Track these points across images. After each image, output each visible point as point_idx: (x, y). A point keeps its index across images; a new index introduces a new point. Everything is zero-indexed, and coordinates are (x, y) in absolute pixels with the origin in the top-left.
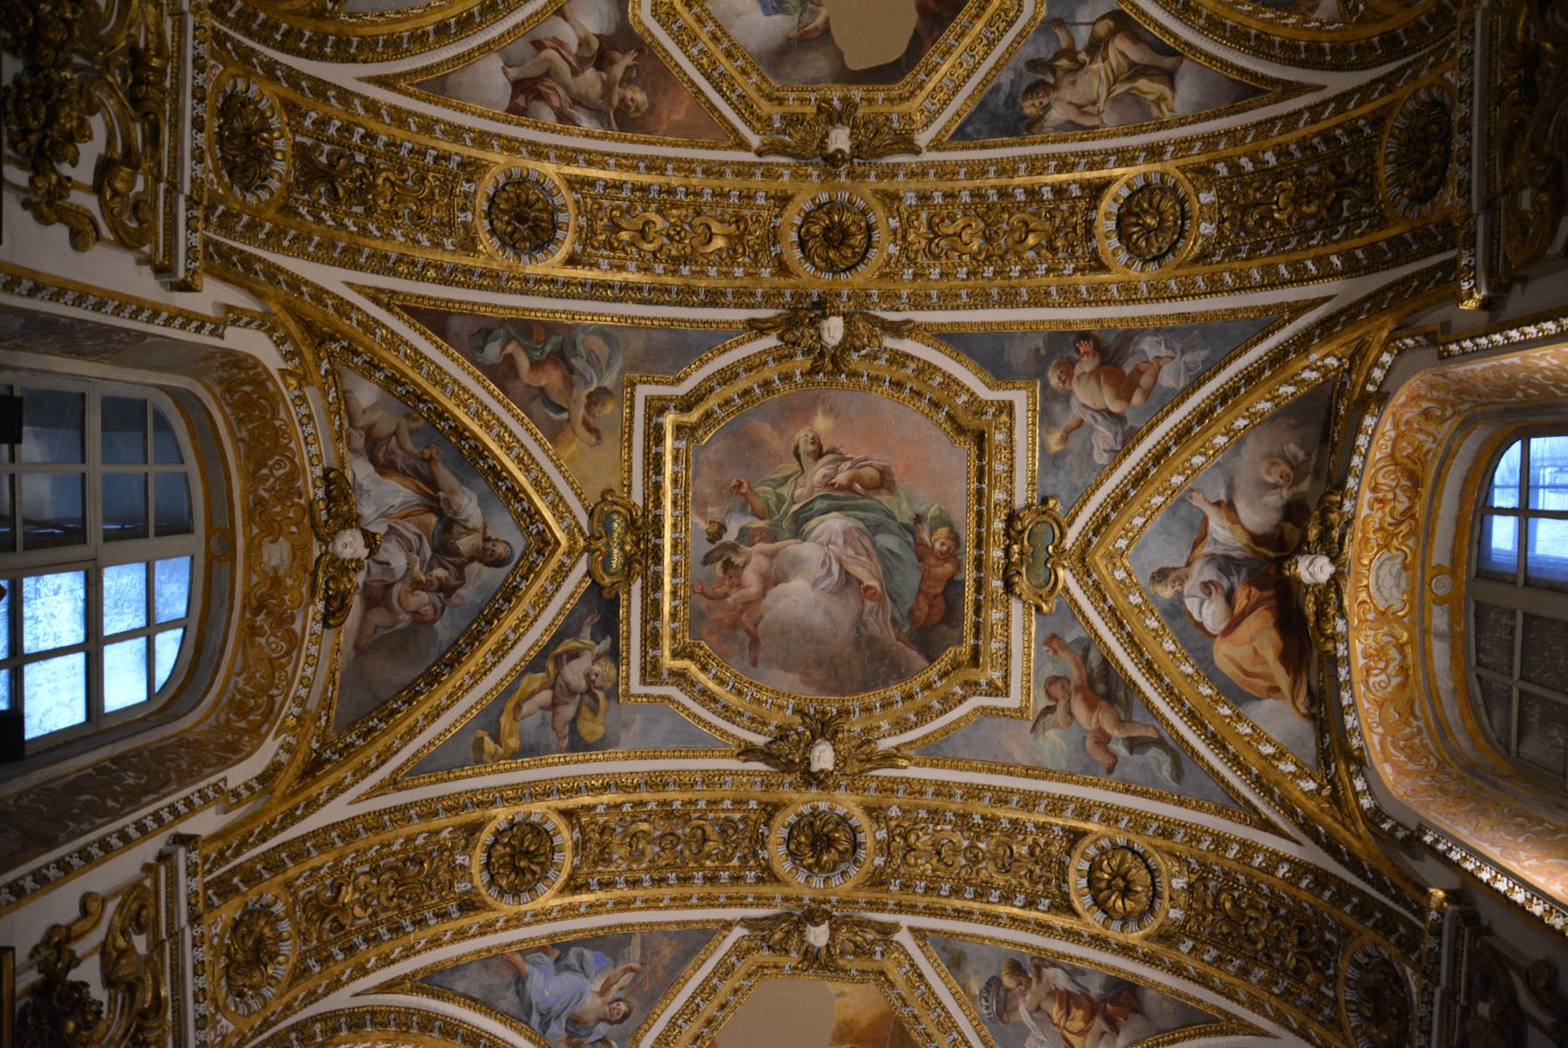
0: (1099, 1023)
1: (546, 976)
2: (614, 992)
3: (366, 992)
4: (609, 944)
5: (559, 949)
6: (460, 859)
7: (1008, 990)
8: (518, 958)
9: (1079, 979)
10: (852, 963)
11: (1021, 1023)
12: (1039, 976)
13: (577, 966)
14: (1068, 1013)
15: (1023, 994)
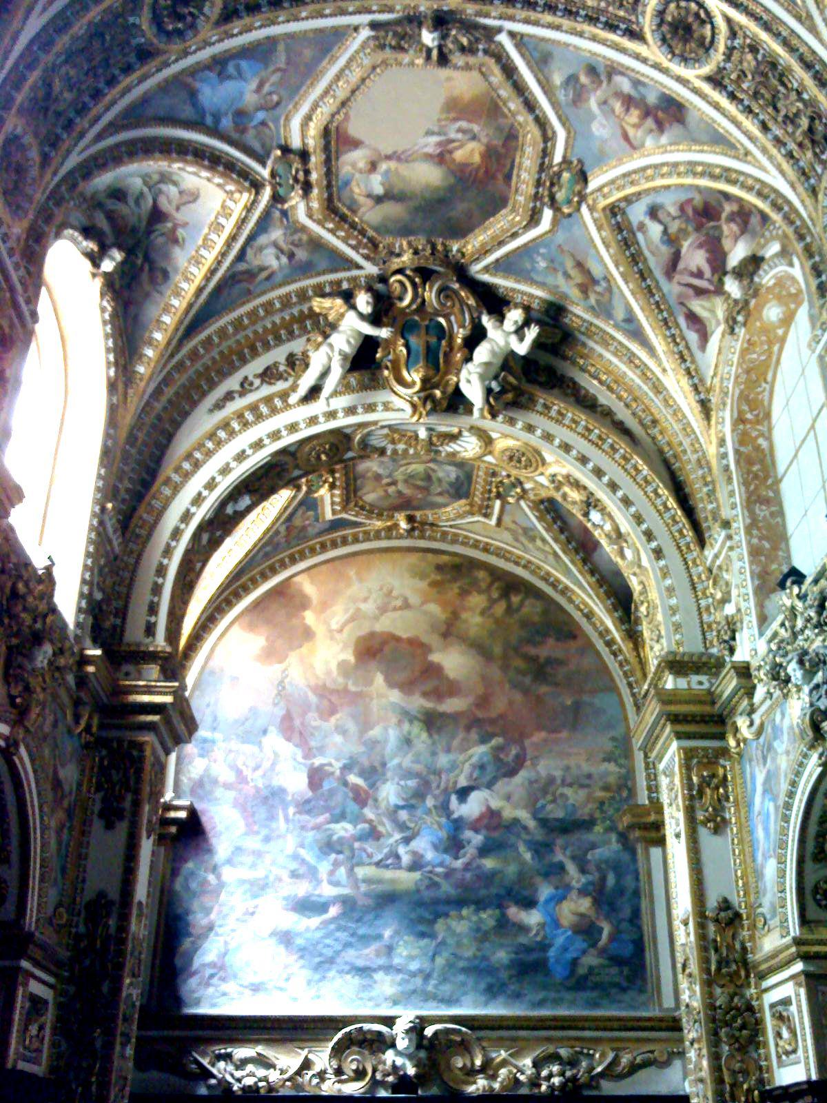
0: (650, 123)
1: (213, 87)
2: (267, 88)
3: (87, 147)
4: (260, 52)
5: (219, 65)
6: (131, 20)
7: (583, 86)
8: (190, 80)
9: (641, 89)
10: (458, 59)
11: (590, 109)
12: (609, 77)
13: (235, 73)
14: (628, 110)
15: (595, 90)
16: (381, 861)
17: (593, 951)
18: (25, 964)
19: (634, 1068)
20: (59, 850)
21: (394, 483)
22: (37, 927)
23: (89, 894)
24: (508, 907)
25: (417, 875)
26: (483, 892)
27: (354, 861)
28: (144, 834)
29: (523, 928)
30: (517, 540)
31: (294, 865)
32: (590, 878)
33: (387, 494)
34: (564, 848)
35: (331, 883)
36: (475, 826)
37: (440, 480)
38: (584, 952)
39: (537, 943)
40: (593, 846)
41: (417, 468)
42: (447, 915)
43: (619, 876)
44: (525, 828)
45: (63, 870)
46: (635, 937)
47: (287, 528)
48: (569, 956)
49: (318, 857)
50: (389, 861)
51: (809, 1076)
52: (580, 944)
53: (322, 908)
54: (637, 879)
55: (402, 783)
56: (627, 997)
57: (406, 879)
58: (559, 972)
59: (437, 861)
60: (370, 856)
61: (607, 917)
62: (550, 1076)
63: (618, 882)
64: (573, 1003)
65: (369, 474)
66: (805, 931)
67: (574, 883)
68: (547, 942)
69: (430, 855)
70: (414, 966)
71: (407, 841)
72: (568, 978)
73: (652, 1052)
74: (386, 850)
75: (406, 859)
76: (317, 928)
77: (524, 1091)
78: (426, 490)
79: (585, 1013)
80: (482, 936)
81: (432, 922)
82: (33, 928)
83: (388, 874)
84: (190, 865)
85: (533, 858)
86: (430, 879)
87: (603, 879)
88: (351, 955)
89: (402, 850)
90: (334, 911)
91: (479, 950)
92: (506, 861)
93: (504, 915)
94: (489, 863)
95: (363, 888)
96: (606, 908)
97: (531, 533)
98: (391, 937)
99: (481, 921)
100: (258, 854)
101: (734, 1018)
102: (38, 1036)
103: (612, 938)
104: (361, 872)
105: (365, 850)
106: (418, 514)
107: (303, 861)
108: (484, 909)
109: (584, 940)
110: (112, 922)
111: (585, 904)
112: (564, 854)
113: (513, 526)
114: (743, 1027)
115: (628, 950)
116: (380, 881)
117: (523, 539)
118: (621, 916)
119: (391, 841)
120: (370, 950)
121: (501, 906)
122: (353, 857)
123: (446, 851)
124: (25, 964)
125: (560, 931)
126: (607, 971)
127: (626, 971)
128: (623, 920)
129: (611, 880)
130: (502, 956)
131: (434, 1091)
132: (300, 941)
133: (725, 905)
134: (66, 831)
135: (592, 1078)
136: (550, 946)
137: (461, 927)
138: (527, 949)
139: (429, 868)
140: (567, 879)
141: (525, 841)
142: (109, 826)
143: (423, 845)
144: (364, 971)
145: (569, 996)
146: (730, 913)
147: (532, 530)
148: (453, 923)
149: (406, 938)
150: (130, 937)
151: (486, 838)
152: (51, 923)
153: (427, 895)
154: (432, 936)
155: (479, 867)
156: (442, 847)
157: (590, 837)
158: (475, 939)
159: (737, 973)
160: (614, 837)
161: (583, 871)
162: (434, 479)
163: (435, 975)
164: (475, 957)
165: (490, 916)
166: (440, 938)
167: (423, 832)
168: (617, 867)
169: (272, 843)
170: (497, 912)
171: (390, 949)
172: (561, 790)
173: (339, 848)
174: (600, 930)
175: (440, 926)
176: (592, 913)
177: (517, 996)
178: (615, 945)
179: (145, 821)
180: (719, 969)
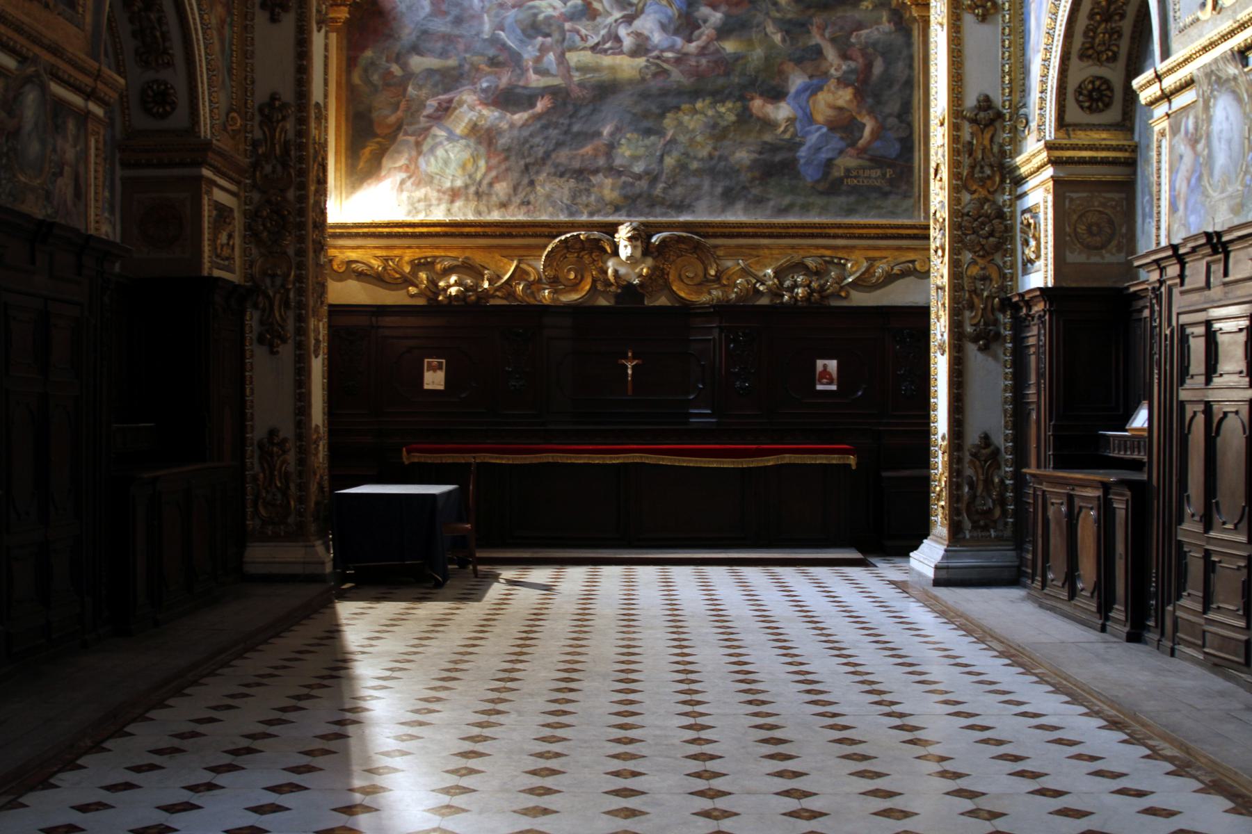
16: (598, 44)
17: (851, 151)
18: (206, 172)
19: (890, 278)
20: (223, 51)
22: (212, 133)
23: (261, 96)
24: (752, 99)
25: (641, 61)
26: (721, 81)
27: (566, 44)
28: (315, 27)
29: (769, 124)
31: (492, 52)
32: (853, 65)
34: (822, 29)
35: (537, 72)
38: (841, 152)
39: (788, 141)
40: (860, 26)
42: (678, 108)
43: (888, 64)
45: (230, 70)
46: (904, 135)
48: (824, 156)
49: (521, 41)
50: (608, 45)
51: (1046, 283)
52: (836, 142)
53: (528, 100)
54: (911, 67)
56: (889, 202)
57: (627, 66)
58: (810, 174)
59: (666, 44)
60: (584, 39)
61: (871, 112)
62: (795, 285)
63: (886, 70)
64: (824, 210)
66: (1062, 134)
67: (832, 71)
68: (798, 139)
69: (657, 37)
70: (638, 168)
71: (629, 20)
72: (818, 181)
73: (913, 262)
74: (603, 32)
75: (628, 42)
76: (523, 125)
77: (764, 301)
79: (839, 220)
80: (718, 133)
81: (662, 116)
82: (209, 137)
83: (607, 60)
84: (369, 53)
85: (784, 40)
86: (657, 65)
87: (869, 66)
88: (563, 156)
89: (623, 31)
90: (540, 106)
91: (715, 149)
92: (750, 42)
93: (746, 109)
94: (730, 47)
95: (577, 77)
96: (870, 101)
98: (612, 134)
99: (721, 116)
100: (449, 39)
101: (983, 224)
102: (228, 244)
103: (876, 135)
104: (573, 58)
105: (578, 32)
107: (504, 47)
108: (723, 102)
109: (842, 138)
110: (290, 125)
111: (845, 97)
112: (823, 35)
114: (991, 234)
115: (894, 150)
116: (597, 69)
118: (887, 110)
119: (610, 20)
120: (588, 149)
121: (742, 98)
122: (564, 39)
123: (676, 32)
124: (206, 172)
125: (814, 127)
126: (867, 173)
127: (889, 172)
128: (890, 115)
129: (878, 68)
130: (743, 156)
131: (663, 301)
132: (503, 141)
133: (986, 103)
134: (227, 28)
135: (842, 288)
136: (801, 144)
137: (693, 122)
138: (774, 148)
139: (655, 53)
140: (824, 66)
141: (775, 20)
142: (274, 19)
143: (648, 24)
144: (581, 174)
145: (821, 201)
146: (991, 113)
148: (686, 119)
149: (628, 135)
150: (311, 141)
151: (727, 16)
152: (225, 129)
153: (655, 85)
154: (660, 132)
155: (717, 51)
156: (672, 26)
157: (857, 15)
158: (712, 136)
159: (989, 177)
160: (885, 16)
161: (845, 56)
163: (664, 178)
164: (711, 157)
165: (729, 110)
166: (668, 138)
167: (648, 10)
168: (888, 52)
169: (465, 25)
170: (739, 104)
171: (611, 147)
173: (547, 31)
174: (864, 125)
175: (669, 121)
176: (853, 107)
177: (759, 201)
178: (877, 144)
179: (314, 10)
180: (971, 174)
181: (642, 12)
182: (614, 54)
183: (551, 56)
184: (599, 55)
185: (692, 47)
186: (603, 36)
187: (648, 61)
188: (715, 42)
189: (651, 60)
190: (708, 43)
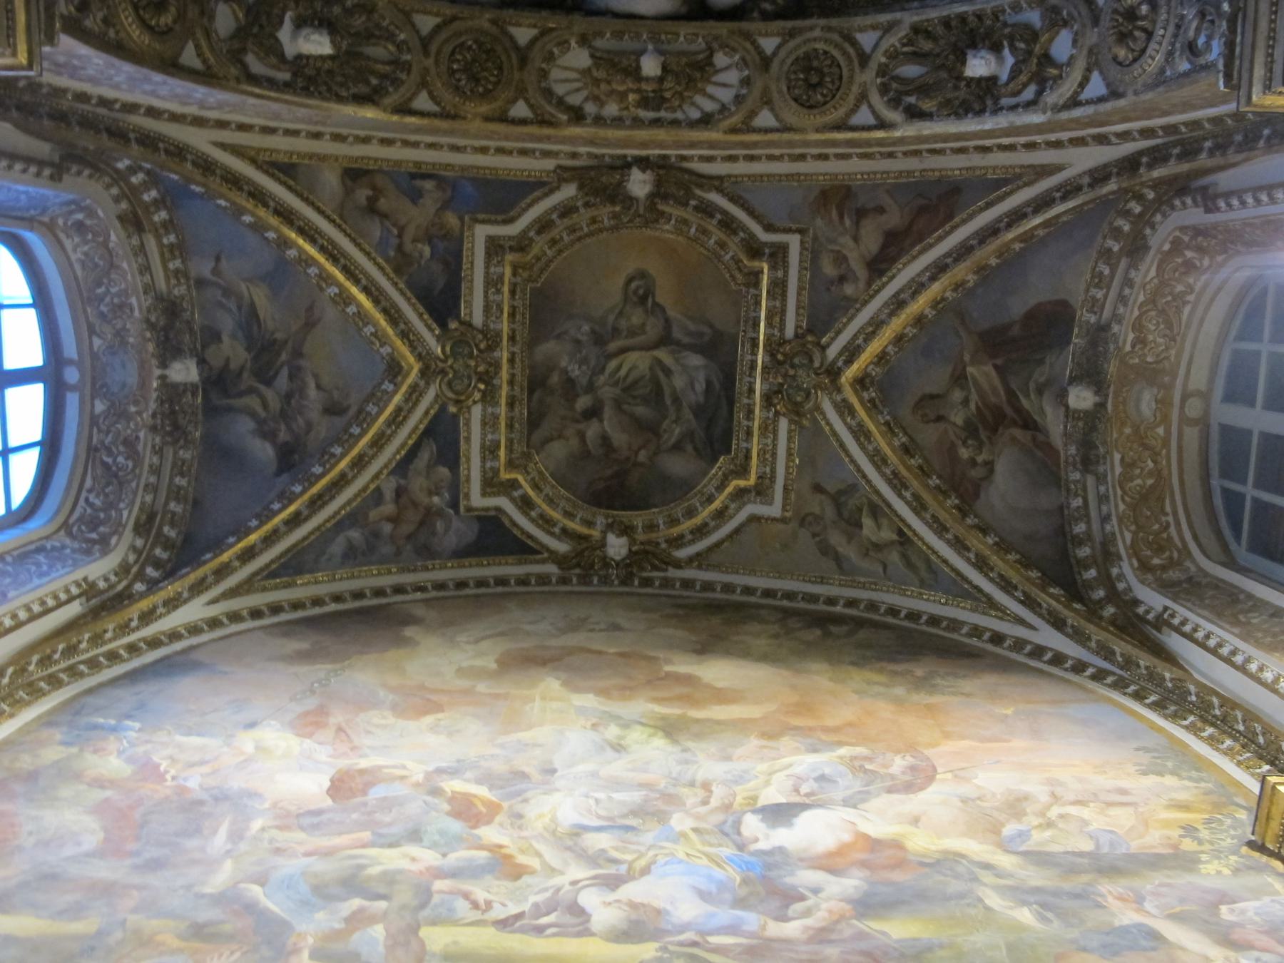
21: (593, 413)
27: (426, 913)
30: (826, 550)
33: (586, 454)
36: (831, 863)
37: (676, 400)
41: (637, 362)
44: (987, 866)
47: (399, 492)
50: (544, 920)
55: (601, 795)
65: (555, 379)
74: (533, 899)
78: (650, 429)
89: (590, 899)
97: (852, 502)
106: (638, 519)
113: (817, 505)
117: (836, 539)
139: (689, 936)
147: (852, 489)
156: (728, 896)
162: (668, 401)
172: (1054, 812)
181: (646, 871)
182: (554, 935)
183: (378, 931)
184: (518, 936)
185: (792, 929)
186: (536, 905)
187: (664, 949)
188: (855, 922)
189: (671, 948)
190: (837, 922)
